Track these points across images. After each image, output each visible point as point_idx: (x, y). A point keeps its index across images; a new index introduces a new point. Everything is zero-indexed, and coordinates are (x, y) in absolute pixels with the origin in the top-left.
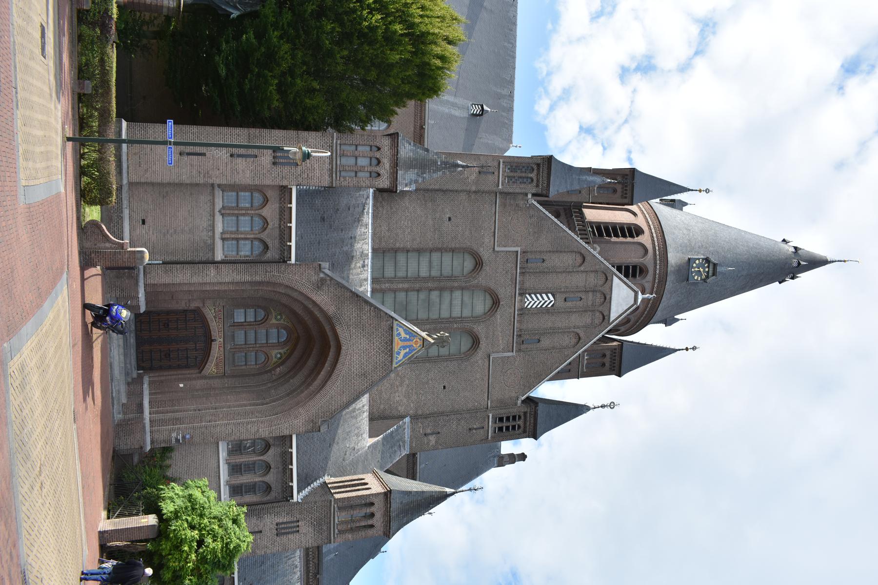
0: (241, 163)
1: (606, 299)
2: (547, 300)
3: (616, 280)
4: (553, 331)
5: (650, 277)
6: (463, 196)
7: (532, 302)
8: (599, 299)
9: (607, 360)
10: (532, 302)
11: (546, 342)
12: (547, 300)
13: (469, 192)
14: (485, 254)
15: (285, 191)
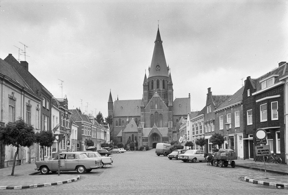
0: (140, 141)
1: (156, 97)
2: (156, 105)
3: (154, 96)
4: (160, 104)
5: (158, 79)
6: (145, 117)
7: (156, 107)
8: (156, 98)
9: (170, 86)
10: (156, 107)
11: (161, 105)
12: (156, 105)
13: (145, 116)
14: (151, 114)
15: (142, 137)
